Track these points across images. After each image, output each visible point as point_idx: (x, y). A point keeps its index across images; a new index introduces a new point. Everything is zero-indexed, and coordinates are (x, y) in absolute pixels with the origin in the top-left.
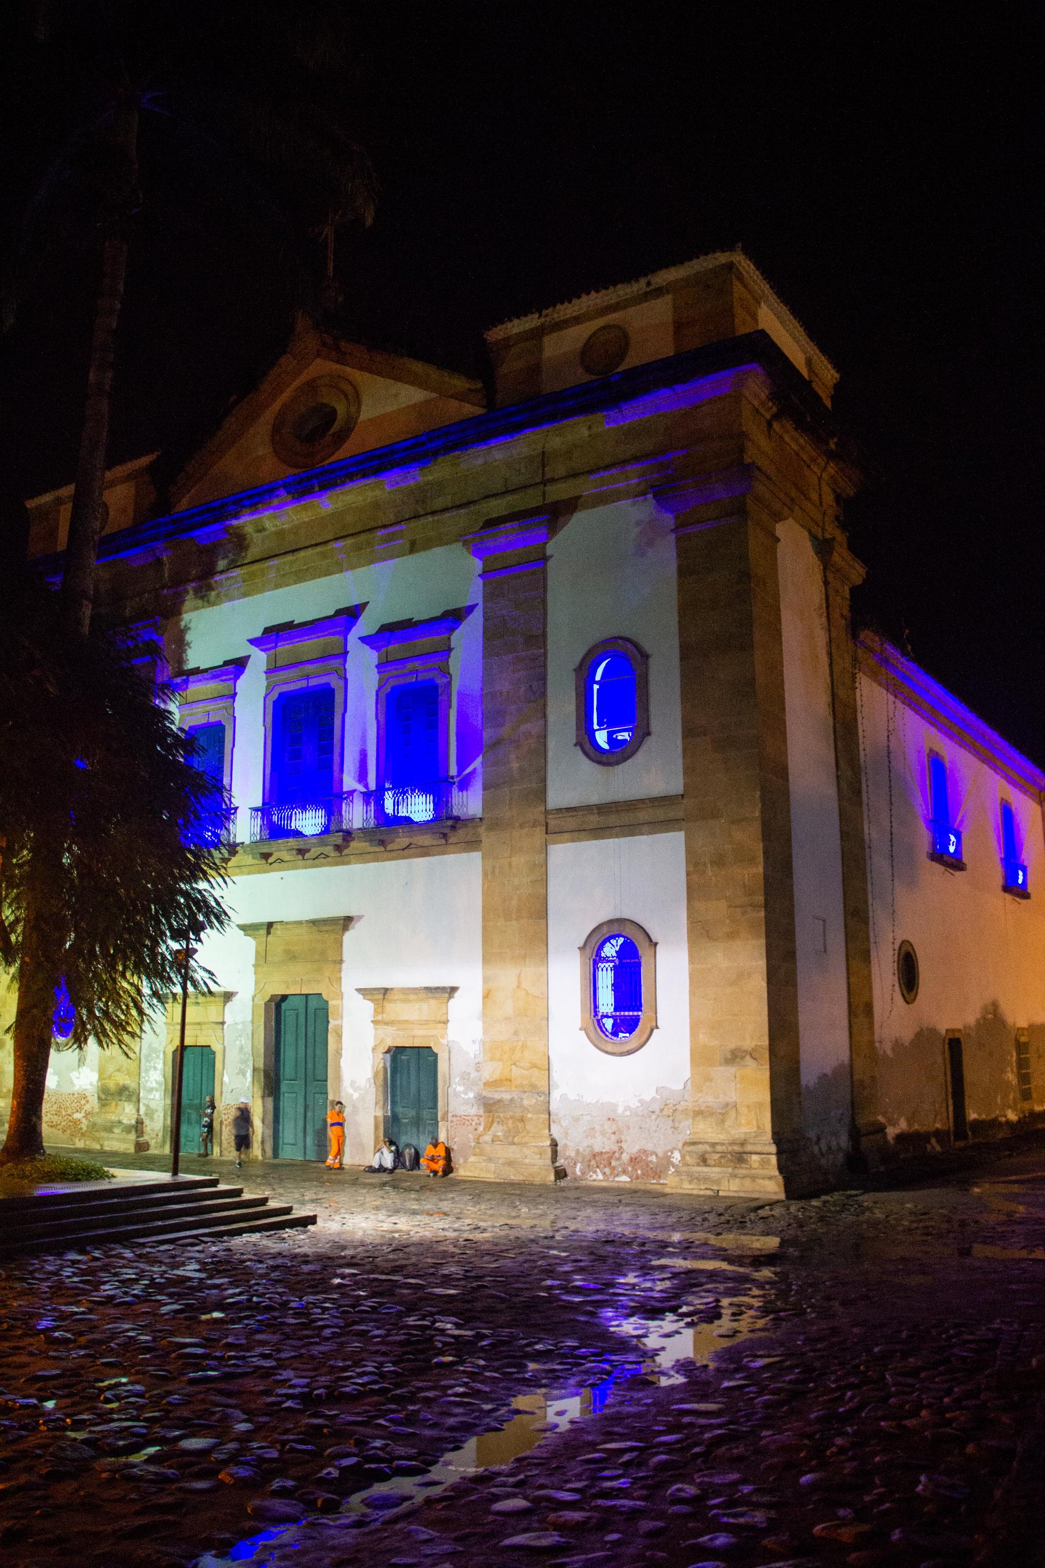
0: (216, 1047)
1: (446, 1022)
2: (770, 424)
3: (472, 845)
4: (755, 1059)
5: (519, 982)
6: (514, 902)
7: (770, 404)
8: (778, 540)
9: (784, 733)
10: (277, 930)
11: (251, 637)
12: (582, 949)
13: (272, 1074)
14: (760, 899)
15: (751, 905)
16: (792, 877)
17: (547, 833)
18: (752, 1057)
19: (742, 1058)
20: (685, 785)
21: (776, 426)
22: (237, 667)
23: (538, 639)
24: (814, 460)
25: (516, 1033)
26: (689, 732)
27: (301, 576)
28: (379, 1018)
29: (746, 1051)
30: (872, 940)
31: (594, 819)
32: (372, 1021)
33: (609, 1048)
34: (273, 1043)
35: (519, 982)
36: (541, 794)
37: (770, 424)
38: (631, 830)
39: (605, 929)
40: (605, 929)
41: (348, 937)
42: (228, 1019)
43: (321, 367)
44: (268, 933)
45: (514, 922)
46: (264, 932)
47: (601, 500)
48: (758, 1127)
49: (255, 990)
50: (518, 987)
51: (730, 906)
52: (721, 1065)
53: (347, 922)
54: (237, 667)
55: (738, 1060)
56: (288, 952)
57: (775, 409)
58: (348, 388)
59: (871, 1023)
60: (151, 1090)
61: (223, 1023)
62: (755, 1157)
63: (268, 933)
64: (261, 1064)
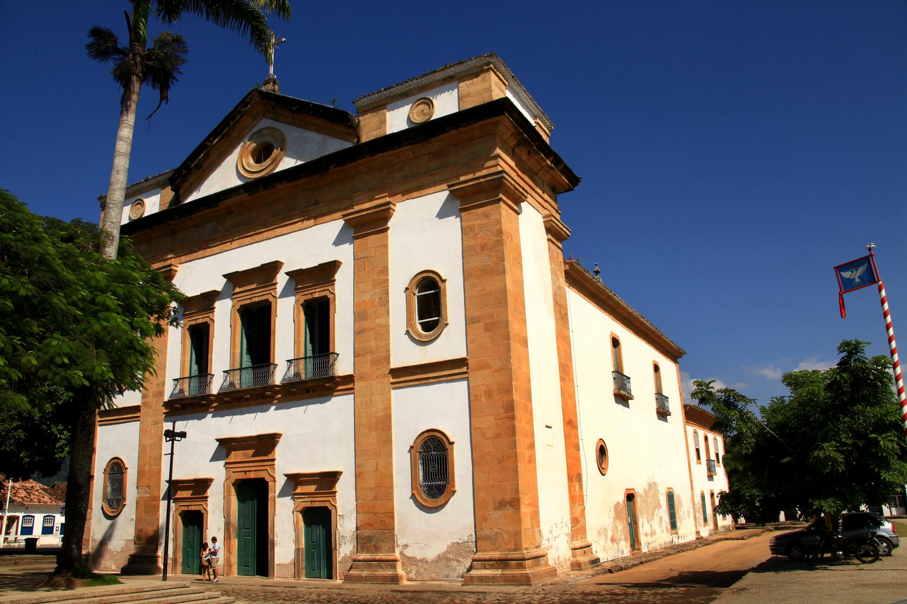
2: (513, 151)
4: (512, 506)
5: (377, 467)
6: (374, 421)
9: (525, 321)
11: (224, 274)
15: (507, 418)
16: (531, 402)
18: (510, 505)
19: (506, 505)
21: (517, 150)
23: (385, 271)
25: (376, 496)
26: (470, 321)
29: (507, 502)
30: (580, 438)
35: (377, 467)
36: (387, 359)
37: (513, 151)
38: (438, 380)
40: (426, 435)
45: (374, 433)
48: (515, 545)
49: (226, 476)
50: (376, 470)
51: (495, 419)
52: (493, 510)
55: (503, 507)
57: (515, 142)
59: (581, 486)
62: (514, 562)
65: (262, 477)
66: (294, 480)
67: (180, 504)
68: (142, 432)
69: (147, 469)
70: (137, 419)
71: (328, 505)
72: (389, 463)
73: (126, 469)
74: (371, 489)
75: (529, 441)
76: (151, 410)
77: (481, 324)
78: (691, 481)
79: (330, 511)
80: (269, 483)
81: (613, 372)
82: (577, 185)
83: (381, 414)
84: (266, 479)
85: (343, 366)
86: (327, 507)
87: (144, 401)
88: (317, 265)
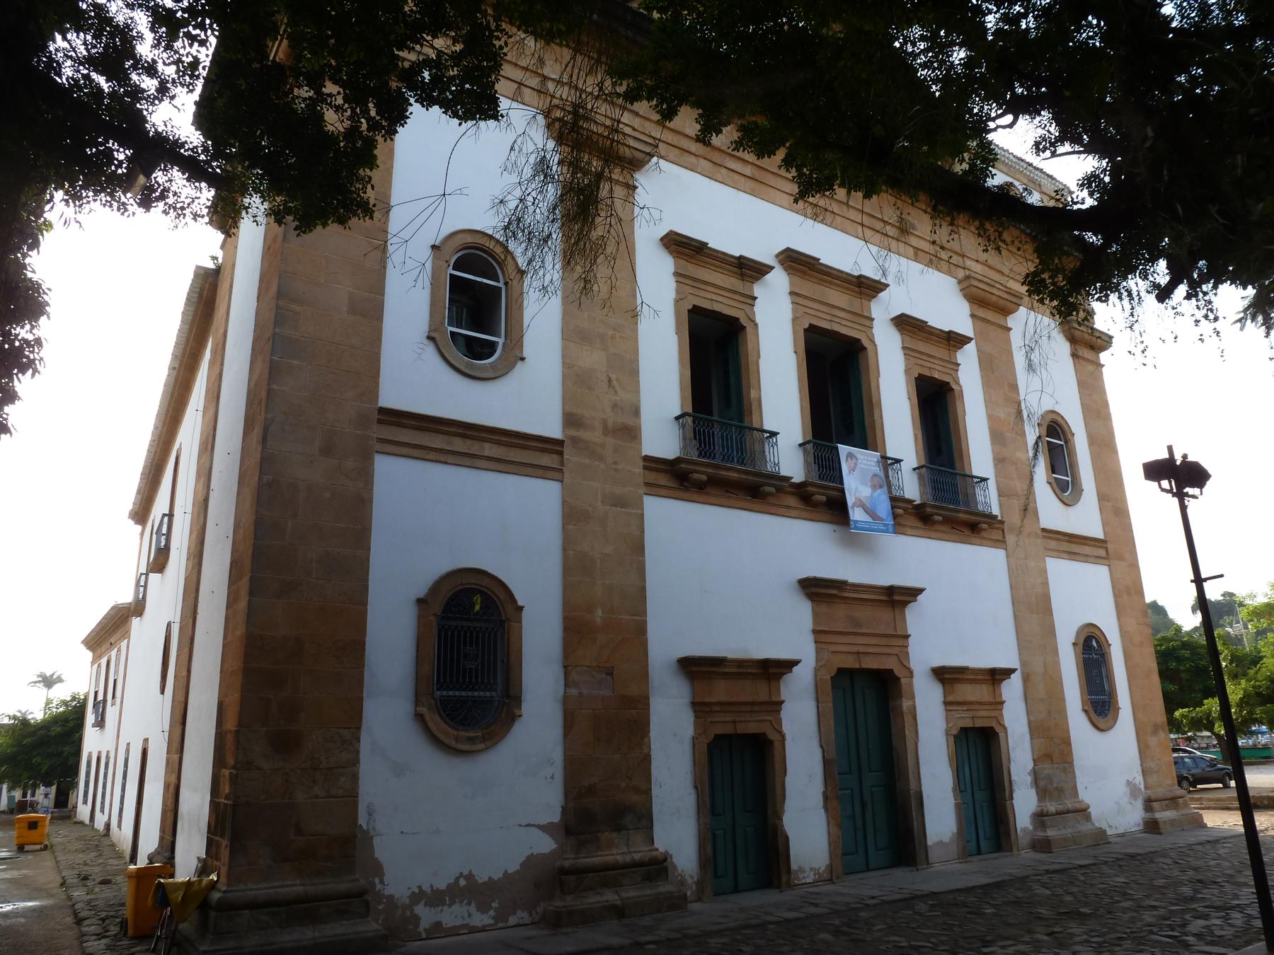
3: (1000, 543)
28: (951, 698)
49: (817, 661)
65: (888, 667)
66: (944, 675)
67: (710, 720)
68: (572, 516)
69: (598, 620)
71: (994, 725)
72: (1057, 664)
73: (521, 608)
74: (1042, 700)
76: (602, 466)
77: (1110, 504)
78: (118, 736)
79: (997, 734)
80: (902, 680)
84: (896, 672)
86: (992, 727)
87: (573, 433)
88: (947, 329)
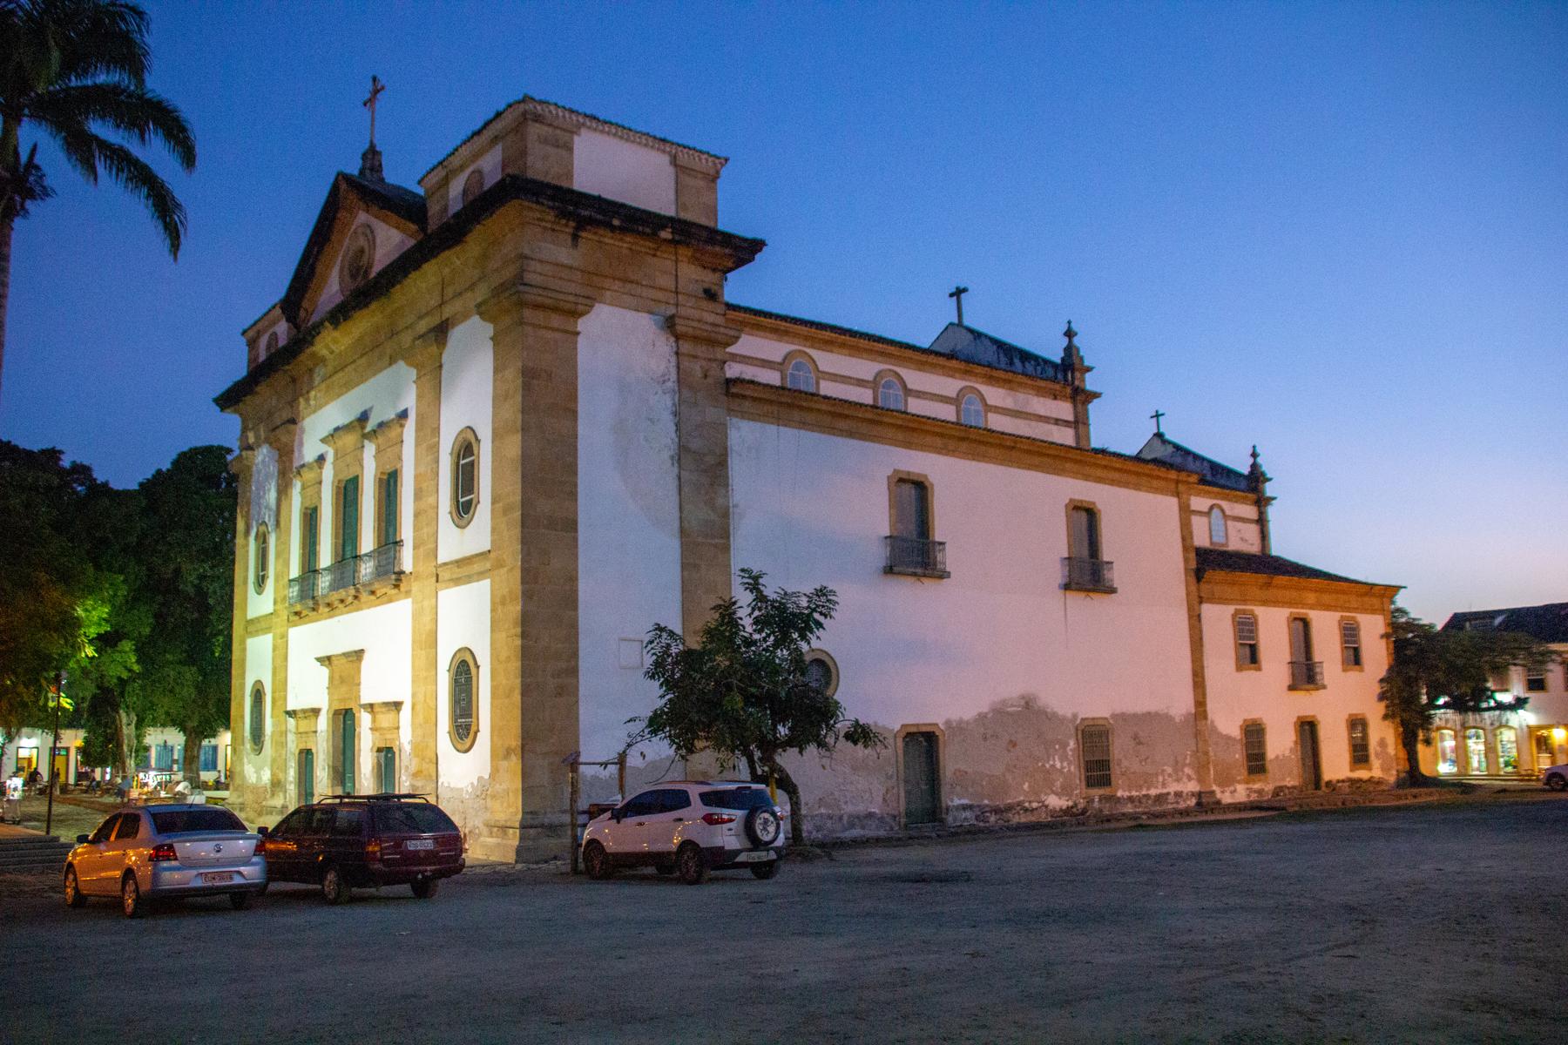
0: (314, 751)
1: (398, 728)
3: (408, 593)
7: (564, 221)
8: (578, 333)
10: (335, 662)
12: (449, 671)
13: (341, 769)
14: (519, 630)
16: (575, 608)
17: (437, 581)
20: (493, 542)
22: (321, 459)
23: (436, 431)
24: (656, 250)
27: (348, 386)
31: (458, 572)
32: (371, 729)
33: (459, 747)
34: (341, 745)
36: (435, 553)
38: (469, 579)
39: (458, 656)
41: (364, 663)
42: (319, 729)
43: (362, 217)
44: (330, 664)
46: (327, 663)
47: (466, 316)
53: (359, 654)
54: (321, 459)
56: (341, 677)
58: (370, 236)
60: (291, 782)
61: (316, 732)
62: (511, 831)
63: (330, 664)
64: (331, 764)
70: (267, 630)
75: (563, 665)
81: (886, 538)
82: (760, 250)
83: (428, 628)
85: (407, 560)
